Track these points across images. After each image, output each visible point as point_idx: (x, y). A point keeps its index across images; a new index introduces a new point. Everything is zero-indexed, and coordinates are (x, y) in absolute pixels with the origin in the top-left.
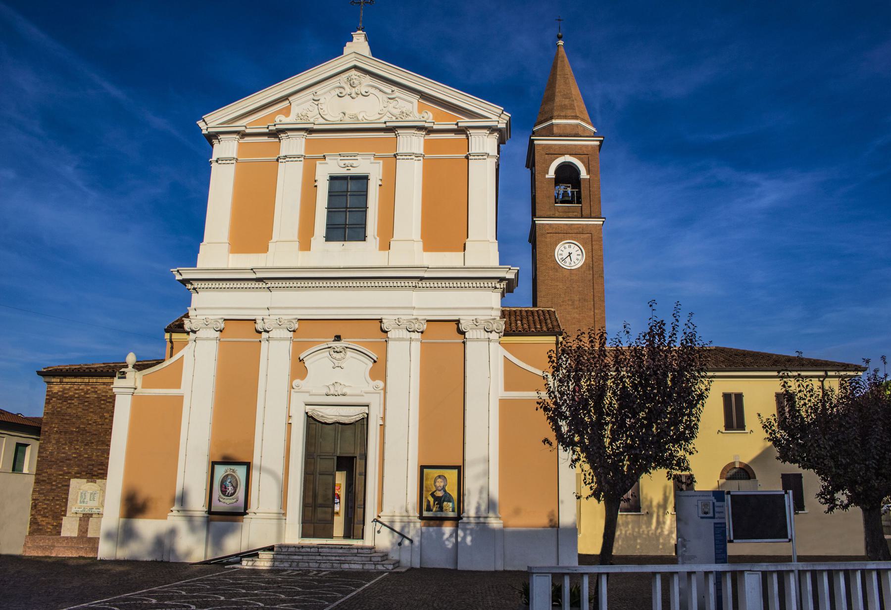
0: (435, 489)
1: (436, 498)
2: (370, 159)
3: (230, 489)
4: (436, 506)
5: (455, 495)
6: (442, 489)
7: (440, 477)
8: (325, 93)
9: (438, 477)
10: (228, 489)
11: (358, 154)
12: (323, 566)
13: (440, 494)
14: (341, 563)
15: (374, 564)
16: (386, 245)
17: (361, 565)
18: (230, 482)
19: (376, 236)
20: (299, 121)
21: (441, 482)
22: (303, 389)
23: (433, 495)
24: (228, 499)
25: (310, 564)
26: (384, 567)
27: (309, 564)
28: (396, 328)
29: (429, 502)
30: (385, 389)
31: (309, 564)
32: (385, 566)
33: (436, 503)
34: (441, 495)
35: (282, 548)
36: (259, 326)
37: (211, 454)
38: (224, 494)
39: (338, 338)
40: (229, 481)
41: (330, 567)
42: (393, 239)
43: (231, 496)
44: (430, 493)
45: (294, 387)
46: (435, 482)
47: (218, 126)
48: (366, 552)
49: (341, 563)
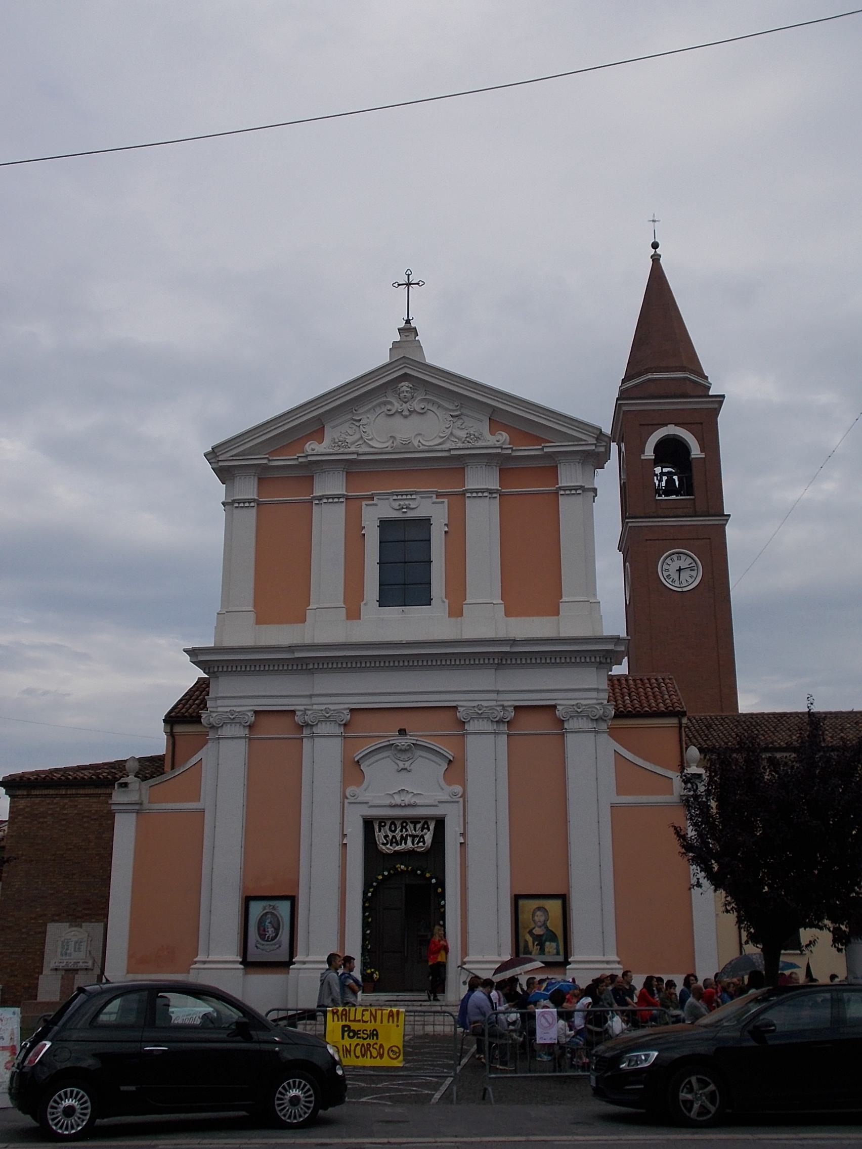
3: (270, 931)
4: (535, 947)
7: (539, 909)
8: (368, 411)
10: (268, 932)
11: (416, 493)
13: (538, 931)
16: (456, 611)
18: (269, 923)
21: (541, 916)
22: (360, 799)
23: (530, 932)
24: (268, 945)
29: (526, 942)
30: (463, 796)
33: (536, 943)
34: (542, 933)
38: (263, 939)
39: (402, 732)
40: (268, 921)
45: (348, 796)
46: (533, 916)
47: (231, 458)
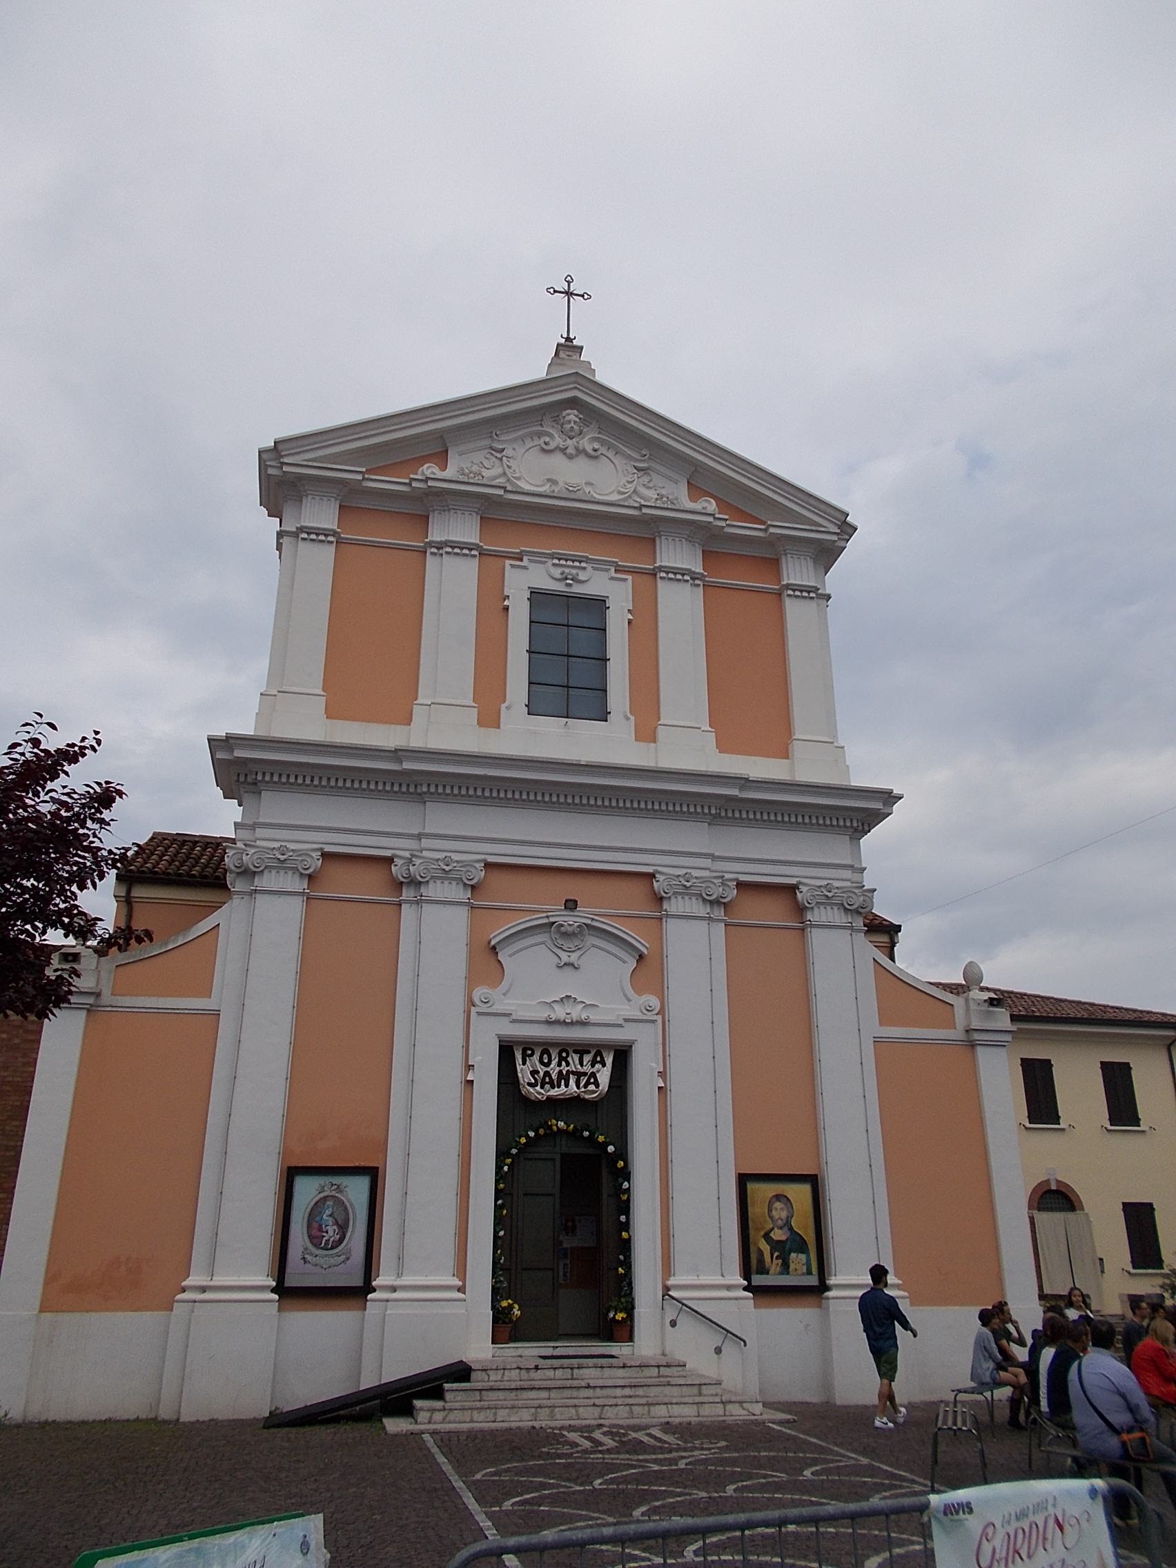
0: (771, 1226)
1: (776, 1245)
2: (608, 570)
3: (332, 1232)
4: (775, 1261)
5: (810, 1238)
6: (785, 1225)
7: (778, 1197)
8: (515, 439)
9: (774, 1199)
10: (327, 1232)
11: (587, 560)
12: (609, 1415)
13: (778, 1235)
14: (649, 1405)
15: (723, 1403)
16: (647, 733)
17: (695, 1406)
18: (330, 1215)
19: (629, 715)
20: (461, 478)
21: (782, 1209)
22: (497, 1008)
23: (767, 1236)
24: (326, 1256)
25: (581, 1410)
26: (744, 1409)
27: (577, 1411)
28: (680, 893)
29: (760, 1252)
30: (661, 1012)
31: (577, 1411)
32: (745, 1405)
33: (776, 1254)
34: (784, 1238)
35: (490, 1373)
36: (397, 870)
37: (285, 1153)
38: (317, 1246)
39: (571, 905)
40: (328, 1212)
41: (626, 1415)
42: (660, 723)
43: (332, 1248)
44: (762, 1233)
45: (477, 1001)
46: (770, 1210)
47: (305, 463)
48: (678, 1374)
49: (649, 1405)
